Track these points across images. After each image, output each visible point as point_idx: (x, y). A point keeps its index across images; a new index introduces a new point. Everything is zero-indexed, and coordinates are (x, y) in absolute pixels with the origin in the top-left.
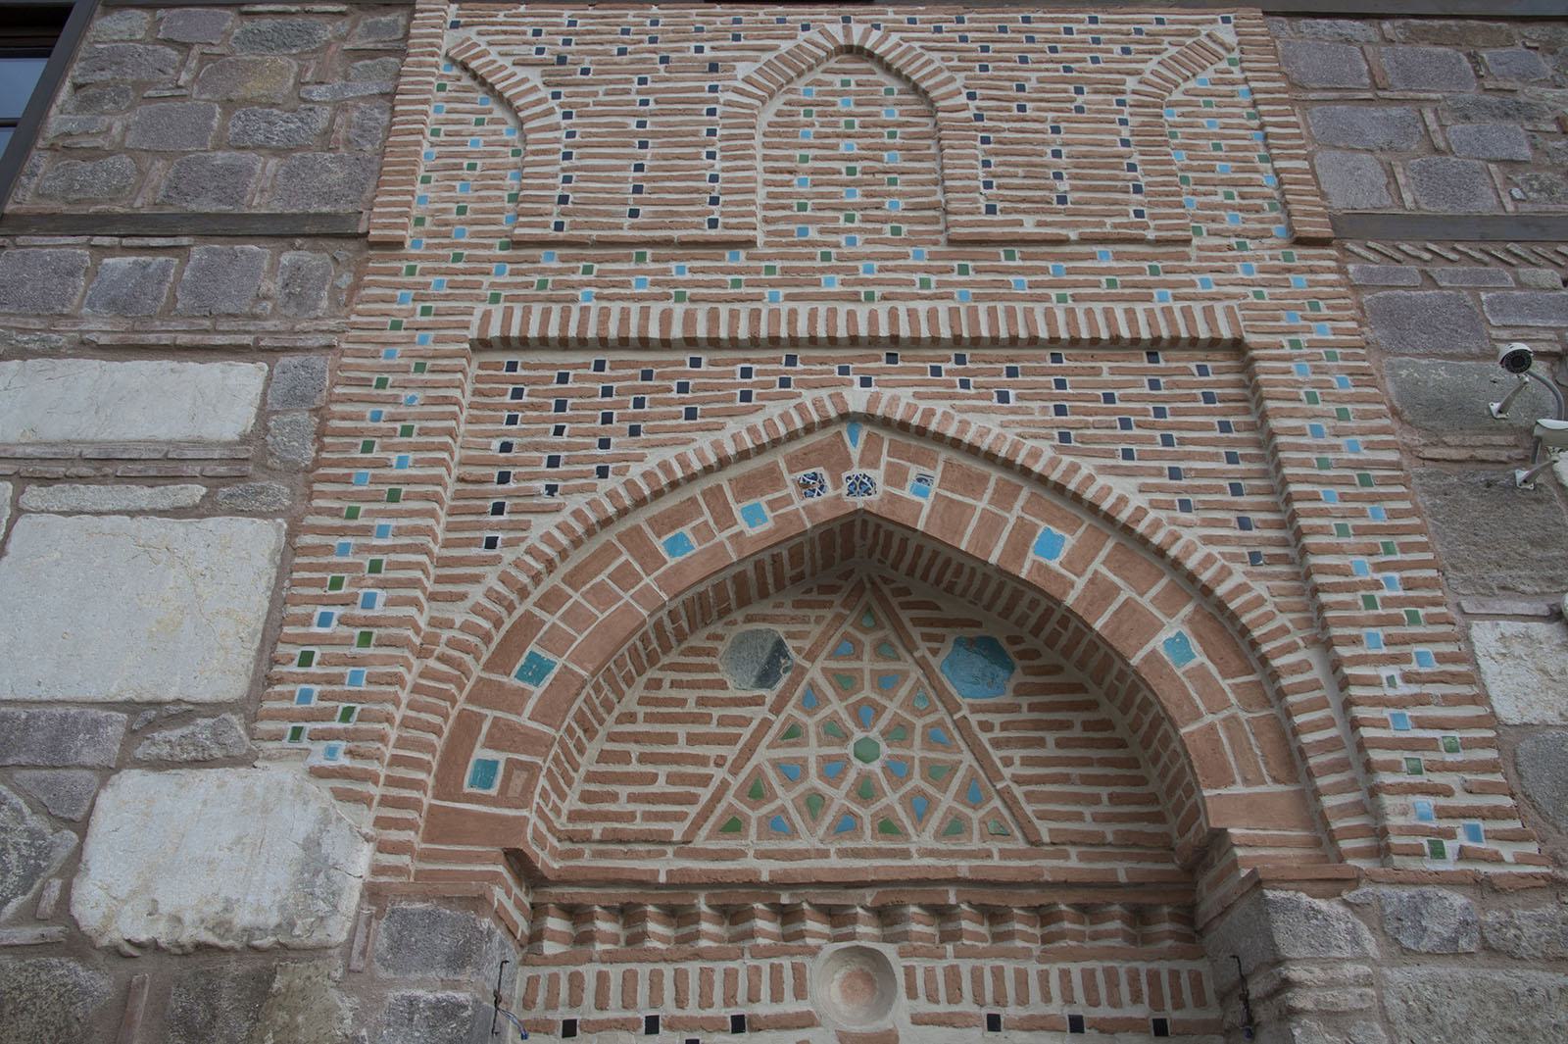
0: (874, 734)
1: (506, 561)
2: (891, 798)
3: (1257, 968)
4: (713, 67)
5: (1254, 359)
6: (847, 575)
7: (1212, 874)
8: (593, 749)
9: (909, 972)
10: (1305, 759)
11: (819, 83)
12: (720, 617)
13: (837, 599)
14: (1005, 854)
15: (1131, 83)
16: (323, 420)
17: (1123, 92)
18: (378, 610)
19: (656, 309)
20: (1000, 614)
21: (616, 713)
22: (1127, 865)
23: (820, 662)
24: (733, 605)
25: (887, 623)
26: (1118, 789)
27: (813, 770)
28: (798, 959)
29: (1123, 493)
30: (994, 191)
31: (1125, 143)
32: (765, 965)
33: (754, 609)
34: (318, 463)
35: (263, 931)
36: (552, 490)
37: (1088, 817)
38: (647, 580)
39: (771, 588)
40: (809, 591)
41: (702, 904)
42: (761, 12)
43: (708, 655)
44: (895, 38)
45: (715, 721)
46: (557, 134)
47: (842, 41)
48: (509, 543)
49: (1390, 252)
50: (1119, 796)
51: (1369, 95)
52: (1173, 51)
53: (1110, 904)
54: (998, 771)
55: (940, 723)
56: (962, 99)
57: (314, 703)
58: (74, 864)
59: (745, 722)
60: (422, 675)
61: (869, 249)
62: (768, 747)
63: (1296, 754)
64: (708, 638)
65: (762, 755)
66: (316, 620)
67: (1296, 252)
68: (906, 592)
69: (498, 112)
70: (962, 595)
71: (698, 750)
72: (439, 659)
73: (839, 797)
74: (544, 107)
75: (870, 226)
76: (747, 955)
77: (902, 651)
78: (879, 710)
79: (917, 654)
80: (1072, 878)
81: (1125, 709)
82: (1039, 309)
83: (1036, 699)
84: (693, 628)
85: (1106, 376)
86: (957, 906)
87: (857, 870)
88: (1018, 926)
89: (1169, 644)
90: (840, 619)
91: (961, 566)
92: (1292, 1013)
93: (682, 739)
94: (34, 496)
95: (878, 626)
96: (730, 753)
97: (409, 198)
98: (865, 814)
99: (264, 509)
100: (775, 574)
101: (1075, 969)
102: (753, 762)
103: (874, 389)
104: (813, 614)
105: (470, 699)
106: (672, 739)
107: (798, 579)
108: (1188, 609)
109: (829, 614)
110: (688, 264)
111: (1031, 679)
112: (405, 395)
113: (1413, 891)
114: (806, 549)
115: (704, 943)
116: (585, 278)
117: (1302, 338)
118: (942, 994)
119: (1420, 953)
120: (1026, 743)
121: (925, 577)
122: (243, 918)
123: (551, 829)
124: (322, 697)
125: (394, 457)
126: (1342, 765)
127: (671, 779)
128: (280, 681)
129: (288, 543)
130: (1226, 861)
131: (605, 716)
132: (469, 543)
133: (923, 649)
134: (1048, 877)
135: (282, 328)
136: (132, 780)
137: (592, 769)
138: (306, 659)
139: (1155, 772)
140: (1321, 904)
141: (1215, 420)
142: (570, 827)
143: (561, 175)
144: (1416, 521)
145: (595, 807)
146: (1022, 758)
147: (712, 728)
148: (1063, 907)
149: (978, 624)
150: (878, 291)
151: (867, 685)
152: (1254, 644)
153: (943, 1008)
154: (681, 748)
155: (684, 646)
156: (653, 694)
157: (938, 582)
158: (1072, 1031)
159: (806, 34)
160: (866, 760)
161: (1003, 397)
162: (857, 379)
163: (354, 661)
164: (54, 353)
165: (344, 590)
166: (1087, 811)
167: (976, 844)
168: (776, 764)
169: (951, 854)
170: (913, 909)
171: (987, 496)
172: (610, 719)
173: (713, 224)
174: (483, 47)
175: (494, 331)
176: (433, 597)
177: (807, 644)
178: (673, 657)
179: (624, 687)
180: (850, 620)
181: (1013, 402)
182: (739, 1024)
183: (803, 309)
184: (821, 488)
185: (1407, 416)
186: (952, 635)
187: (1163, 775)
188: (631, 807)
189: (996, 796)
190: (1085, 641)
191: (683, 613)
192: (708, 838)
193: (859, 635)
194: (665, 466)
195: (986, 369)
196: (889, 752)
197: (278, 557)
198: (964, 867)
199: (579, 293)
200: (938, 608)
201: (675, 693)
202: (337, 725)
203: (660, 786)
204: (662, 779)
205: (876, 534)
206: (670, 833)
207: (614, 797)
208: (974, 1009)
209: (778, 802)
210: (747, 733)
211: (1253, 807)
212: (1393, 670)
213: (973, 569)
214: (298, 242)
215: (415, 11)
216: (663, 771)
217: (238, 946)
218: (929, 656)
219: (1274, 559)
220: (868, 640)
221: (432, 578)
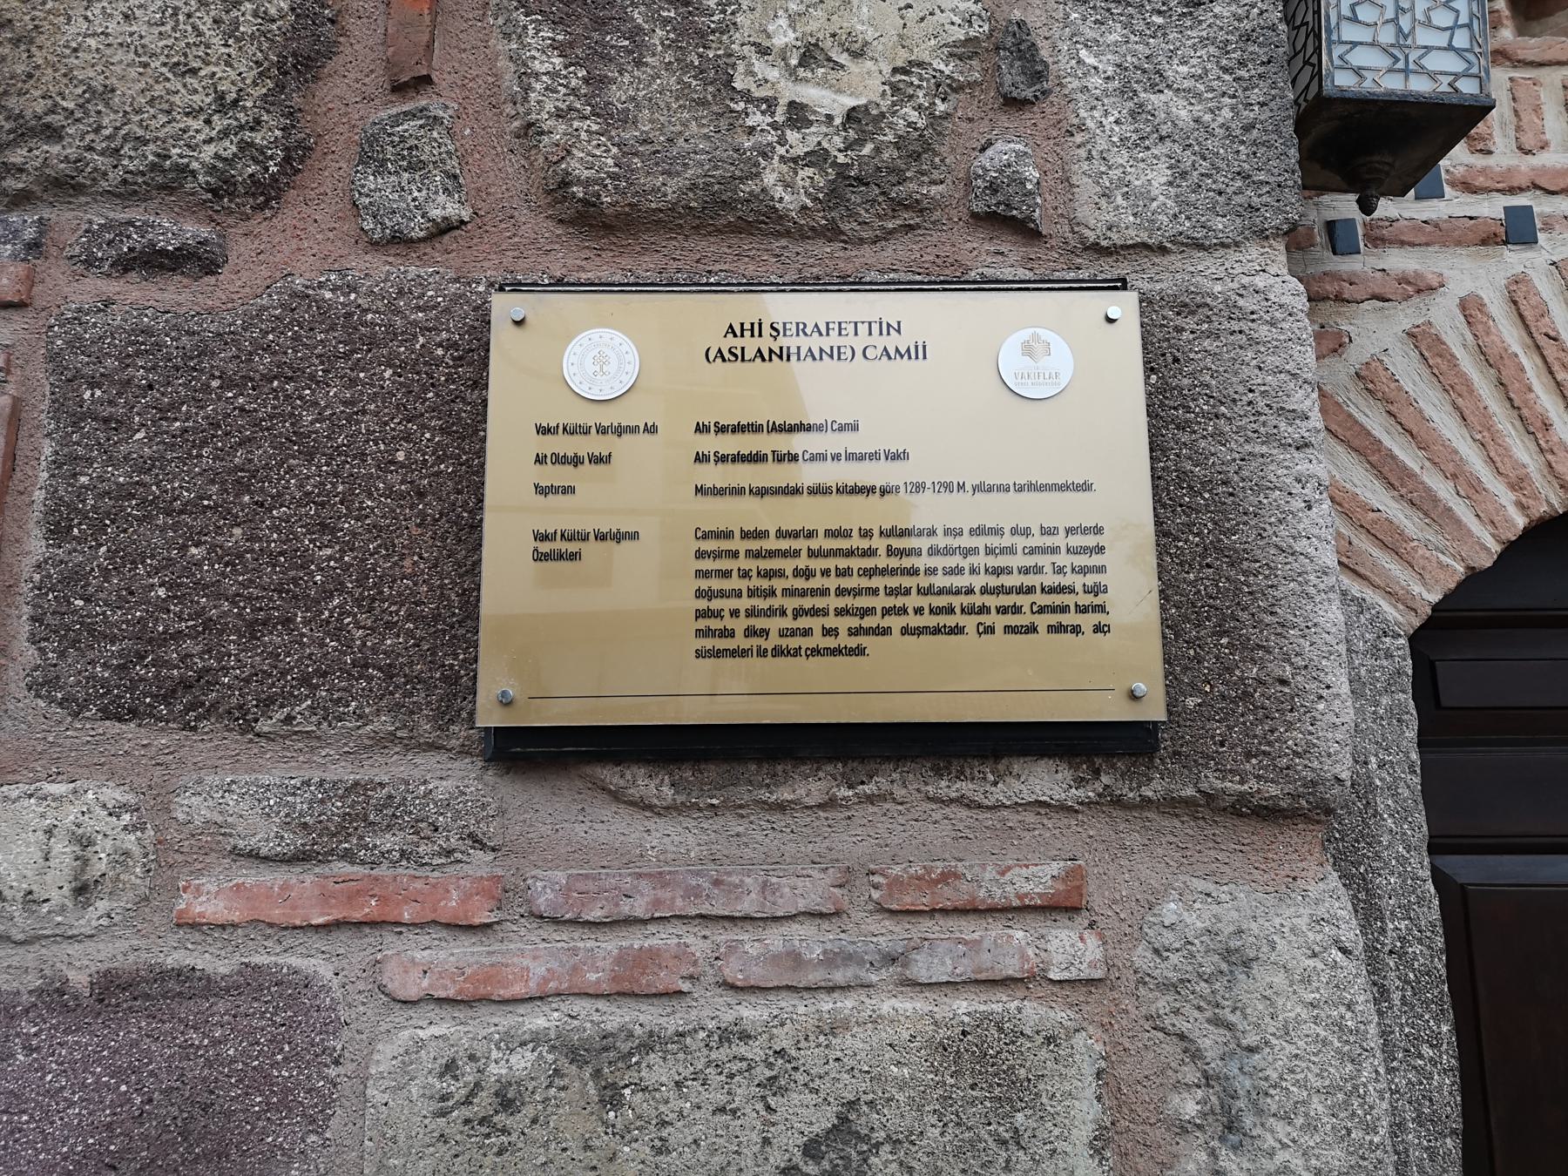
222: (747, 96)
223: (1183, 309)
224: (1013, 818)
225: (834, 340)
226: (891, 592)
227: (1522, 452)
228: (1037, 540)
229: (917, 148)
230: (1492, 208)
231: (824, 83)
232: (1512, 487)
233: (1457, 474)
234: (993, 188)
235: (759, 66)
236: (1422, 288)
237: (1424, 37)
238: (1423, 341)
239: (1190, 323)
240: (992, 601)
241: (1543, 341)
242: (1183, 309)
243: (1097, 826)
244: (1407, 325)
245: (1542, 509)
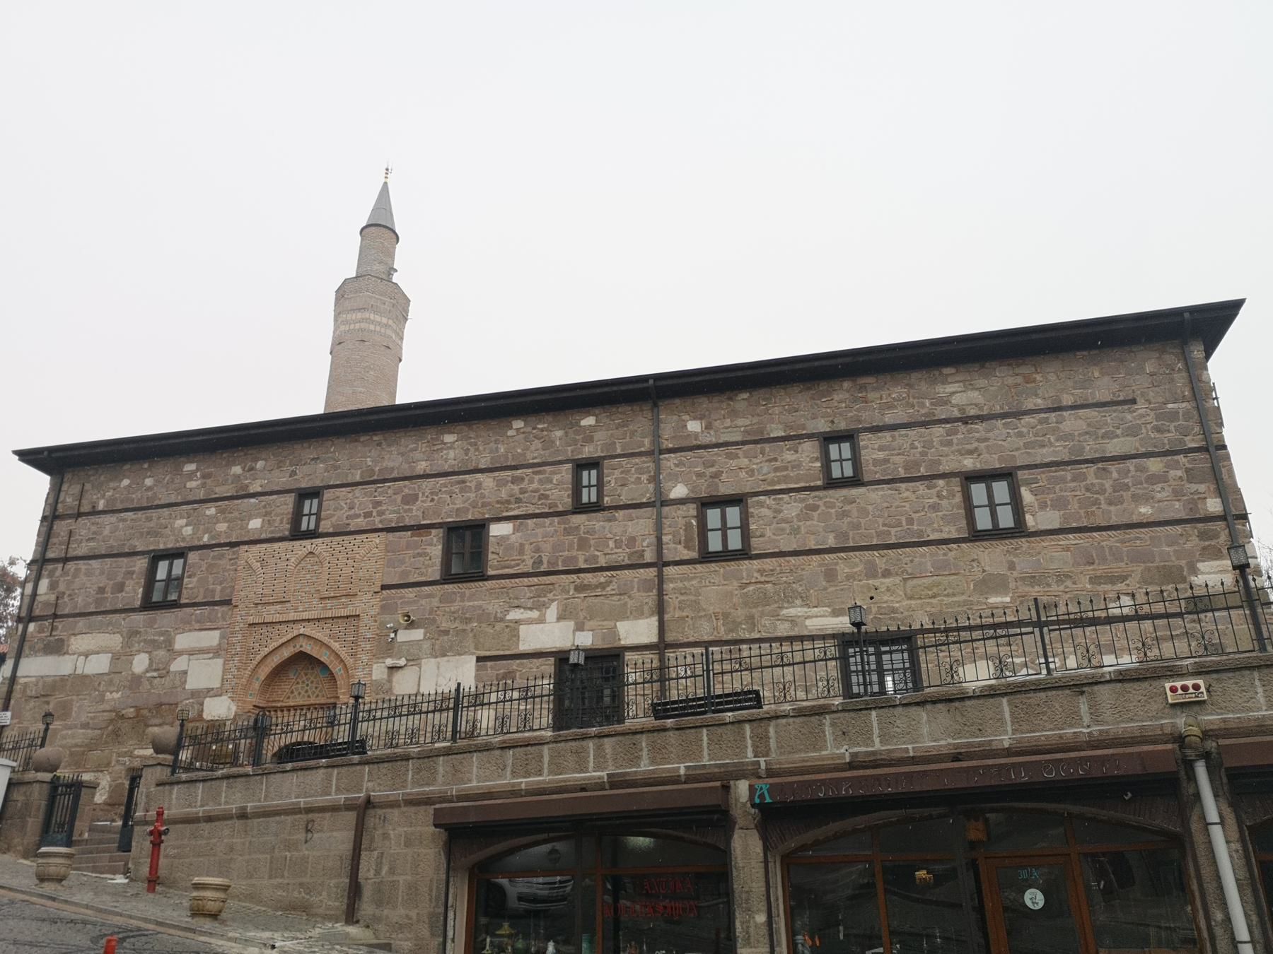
15: (358, 556)
18: (236, 673)
29: (336, 646)
58: (202, 710)
73: (303, 693)
94: (191, 657)
136: (207, 699)
164: (190, 631)
195: (322, 623)
198: (318, 702)
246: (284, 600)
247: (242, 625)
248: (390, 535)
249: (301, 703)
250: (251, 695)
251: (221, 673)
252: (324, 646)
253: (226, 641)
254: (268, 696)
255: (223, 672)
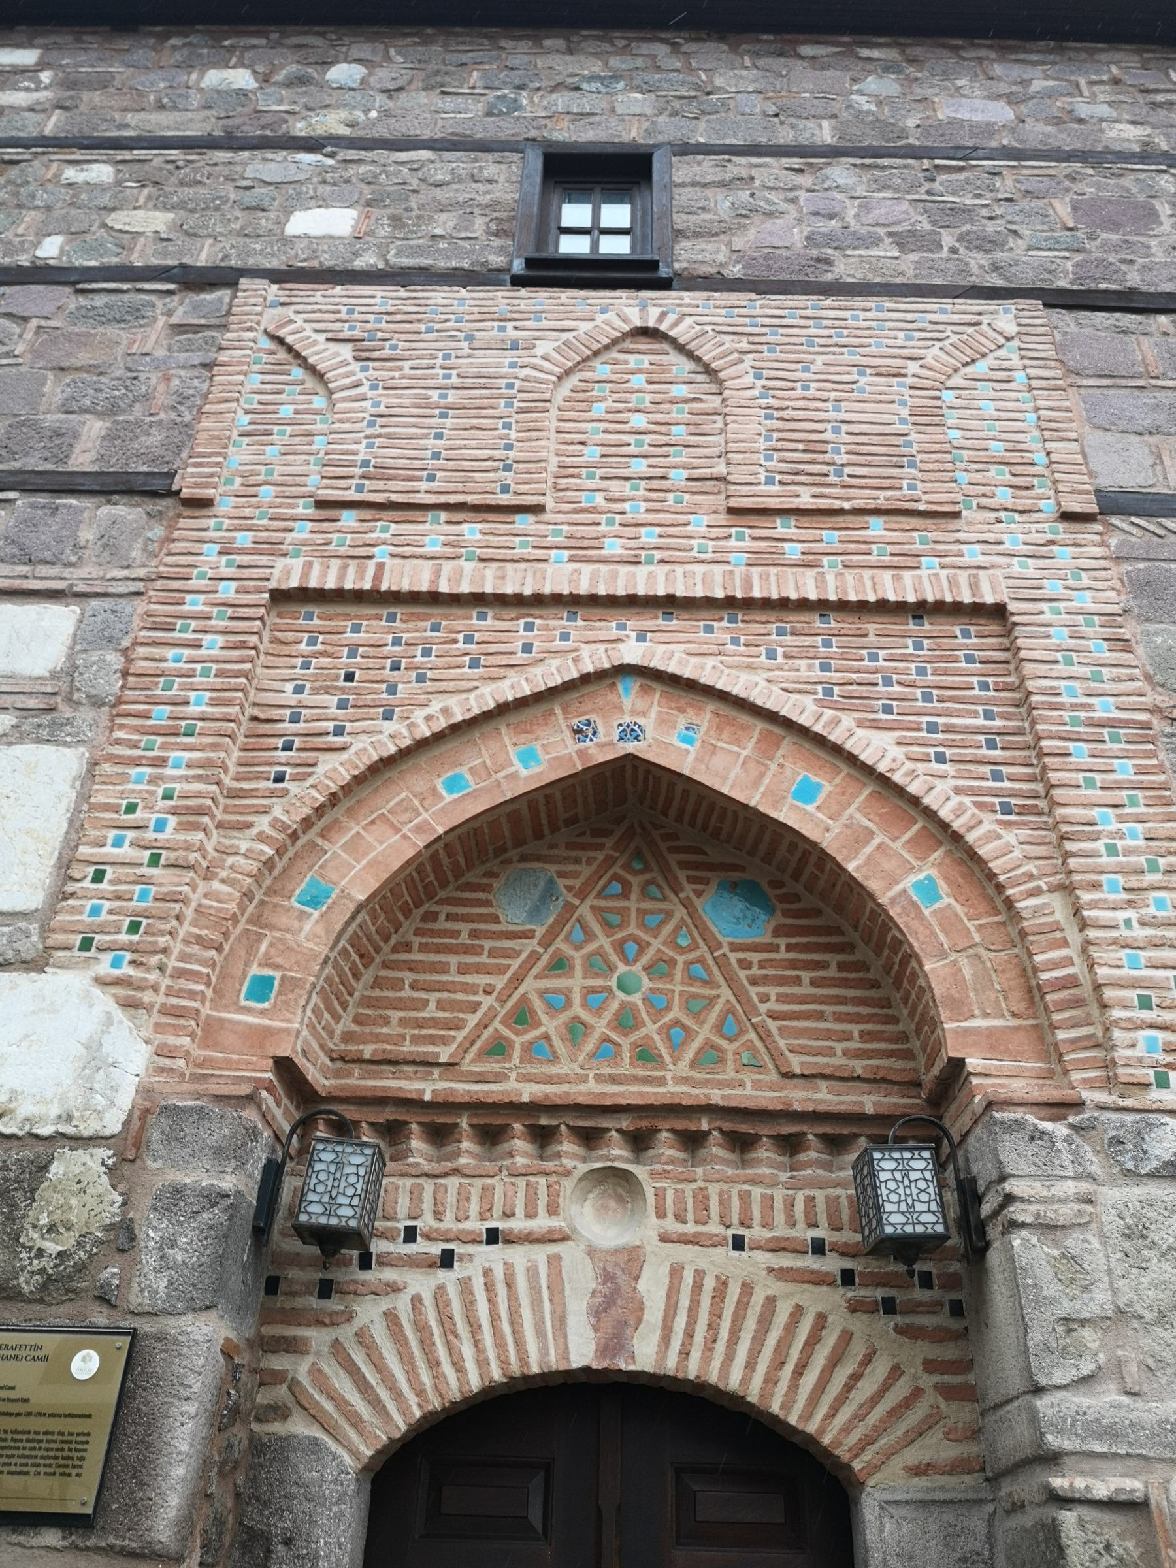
0: (637, 968)
1: (292, 794)
2: (650, 1028)
3: (988, 1188)
4: (515, 346)
5: (1015, 624)
6: (619, 821)
7: (953, 1107)
8: (368, 976)
9: (660, 1194)
10: (1042, 997)
11: (616, 362)
12: (496, 856)
13: (609, 842)
14: (757, 1085)
16: (129, 661)
17: (905, 375)
18: (168, 834)
19: (447, 567)
20: (763, 860)
21: (393, 941)
22: (873, 1098)
23: (589, 902)
24: (509, 844)
25: (655, 868)
26: (869, 1027)
27: (577, 999)
28: (553, 1178)
30: (774, 463)
31: (903, 421)
32: (521, 1182)
33: (525, 849)
34: (119, 701)
35: (41, 1119)
36: (339, 731)
37: (839, 1052)
38: (425, 815)
39: (546, 830)
40: (583, 834)
41: (464, 1123)
42: (563, 296)
43: (483, 891)
44: (689, 321)
45: (486, 952)
46: (363, 404)
47: (638, 323)
48: (295, 778)
49: (1152, 527)
50: (869, 1033)
51: (1141, 383)
52: (954, 338)
53: (857, 1136)
54: (754, 1006)
55: (701, 961)
56: (749, 379)
57: (104, 916)
59: (513, 954)
60: (206, 896)
61: (651, 517)
62: (536, 978)
63: (1036, 991)
64: (484, 875)
65: (529, 985)
66: (110, 841)
67: (1061, 526)
68: (674, 836)
69: (310, 383)
70: (728, 842)
71: (468, 979)
72: (223, 881)
74: (353, 379)
75: (654, 495)
76: (505, 1173)
77: (668, 892)
78: (643, 947)
79: (682, 895)
80: (821, 1108)
81: (878, 953)
82: (811, 573)
83: (793, 940)
84: (470, 866)
85: (872, 638)
86: (709, 1133)
87: (614, 1095)
88: (766, 1154)
89: (918, 885)
90: (610, 862)
91: (724, 810)
92: (1014, 1225)
93: (453, 969)
95: (647, 869)
96: (500, 982)
97: (220, 459)
98: (625, 1043)
99: (68, 739)
100: (549, 816)
101: (820, 1195)
102: (521, 990)
103: (648, 644)
104: (584, 855)
105: (249, 921)
106: (443, 969)
107: (571, 821)
108: (938, 854)
109: (600, 856)
110: (479, 526)
111: (789, 921)
112: (207, 639)
113: (1138, 1116)
114: (579, 791)
115: (463, 1161)
116: (383, 536)
117: (1062, 605)
118: (690, 1216)
119: (1140, 1175)
120: (782, 981)
121: (692, 824)
122: (25, 1109)
123: (322, 1046)
124: (110, 912)
125: (192, 695)
126: (1077, 1003)
127: (440, 1006)
128: (72, 895)
129: (88, 771)
130: (965, 1091)
131: (382, 944)
132: (259, 777)
133: (688, 890)
134: (797, 1107)
135: (94, 575)
137: (366, 993)
138: (99, 877)
139: (905, 1012)
140: (1047, 1126)
141: (975, 679)
142: (343, 1047)
143: (365, 442)
144: (1161, 778)
145: (367, 1030)
146: (778, 995)
147: (484, 959)
148: (810, 1137)
149: (743, 869)
150: (658, 555)
151: (633, 922)
152: (1000, 888)
153: (690, 1228)
154: (453, 977)
155: (462, 880)
156: (430, 926)
157: (705, 828)
158: (814, 1253)
159: (605, 316)
160: (627, 992)
161: (772, 655)
162: (634, 634)
163: (142, 880)
165: (139, 814)
166: (839, 1047)
167: (729, 1073)
168: (542, 993)
169: (705, 1083)
170: (665, 1135)
171: (750, 745)
172: (386, 948)
173: (505, 489)
174: (300, 323)
175: (294, 583)
176: (220, 826)
177: (577, 883)
178: (449, 892)
179: (401, 917)
180: (620, 862)
181: (780, 660)
182: (493, 1236)
183: (587, 569)
184: (595, 733)
185: (1158, 678)
186: (715, 878)
187: (912, 1014)
188: (401, 1030)
189: (751, 1029)
190: (840, 884)
191: (459, 847)
192: (473, 1061)
193: (629, 877)
194: (445, 711)
196: (651, 985)
197: (78, 784)
198: (716, 1096)
199: (376, 550)
200: (705, 854)
201: (450, 925)
202: (124, 937)
203: (430, 1012)
204: (432, 1005)
205: (646, 779)
206: (438, 1054)
207: (387, 1021)
208: (720, 1230)
209: (543, 1029)
210: (515, 964)
211: (993, 1042)
212: (1131, 914)
213: (735, 813)
214: (116, 497)
215: (238, 290)
216: (433, 997)
217: (21, 1133)
218: (692, 896)
219: (1023, 811)
220: (636, 881)
221: (221, 807)
222: (23, 1246)
223: (159, 1339)
224: (37, 1552)
225: (17, 1352)
226: (8, 1456)
227: (426, 1378)
228: (66, 1438)
229: (81, 1268)
230: (436, 1249)
231: (53, 1241)
232: (417, 1395)
233: (393, 1388)
234: (101, 1287)
235: (31, 1232)
236: (395, 1289)
237: (342, 1200)
238: (391, 1318)
239: (159, 1345)
240: (43, 1462)
241: (446, 1320)
242: (159, 1339)
243: (68, 1558)
244: (384, 1308)
245: (430, 1408)
246: (505, 499)
247: (227, 591)
248: (1066, 319)
249: (590, 1090)
250: (261, 988)
251: (56, 827)
252: (788, 745)
253: (115, 660)
254: (346, 1023)
255: (76, 827)
